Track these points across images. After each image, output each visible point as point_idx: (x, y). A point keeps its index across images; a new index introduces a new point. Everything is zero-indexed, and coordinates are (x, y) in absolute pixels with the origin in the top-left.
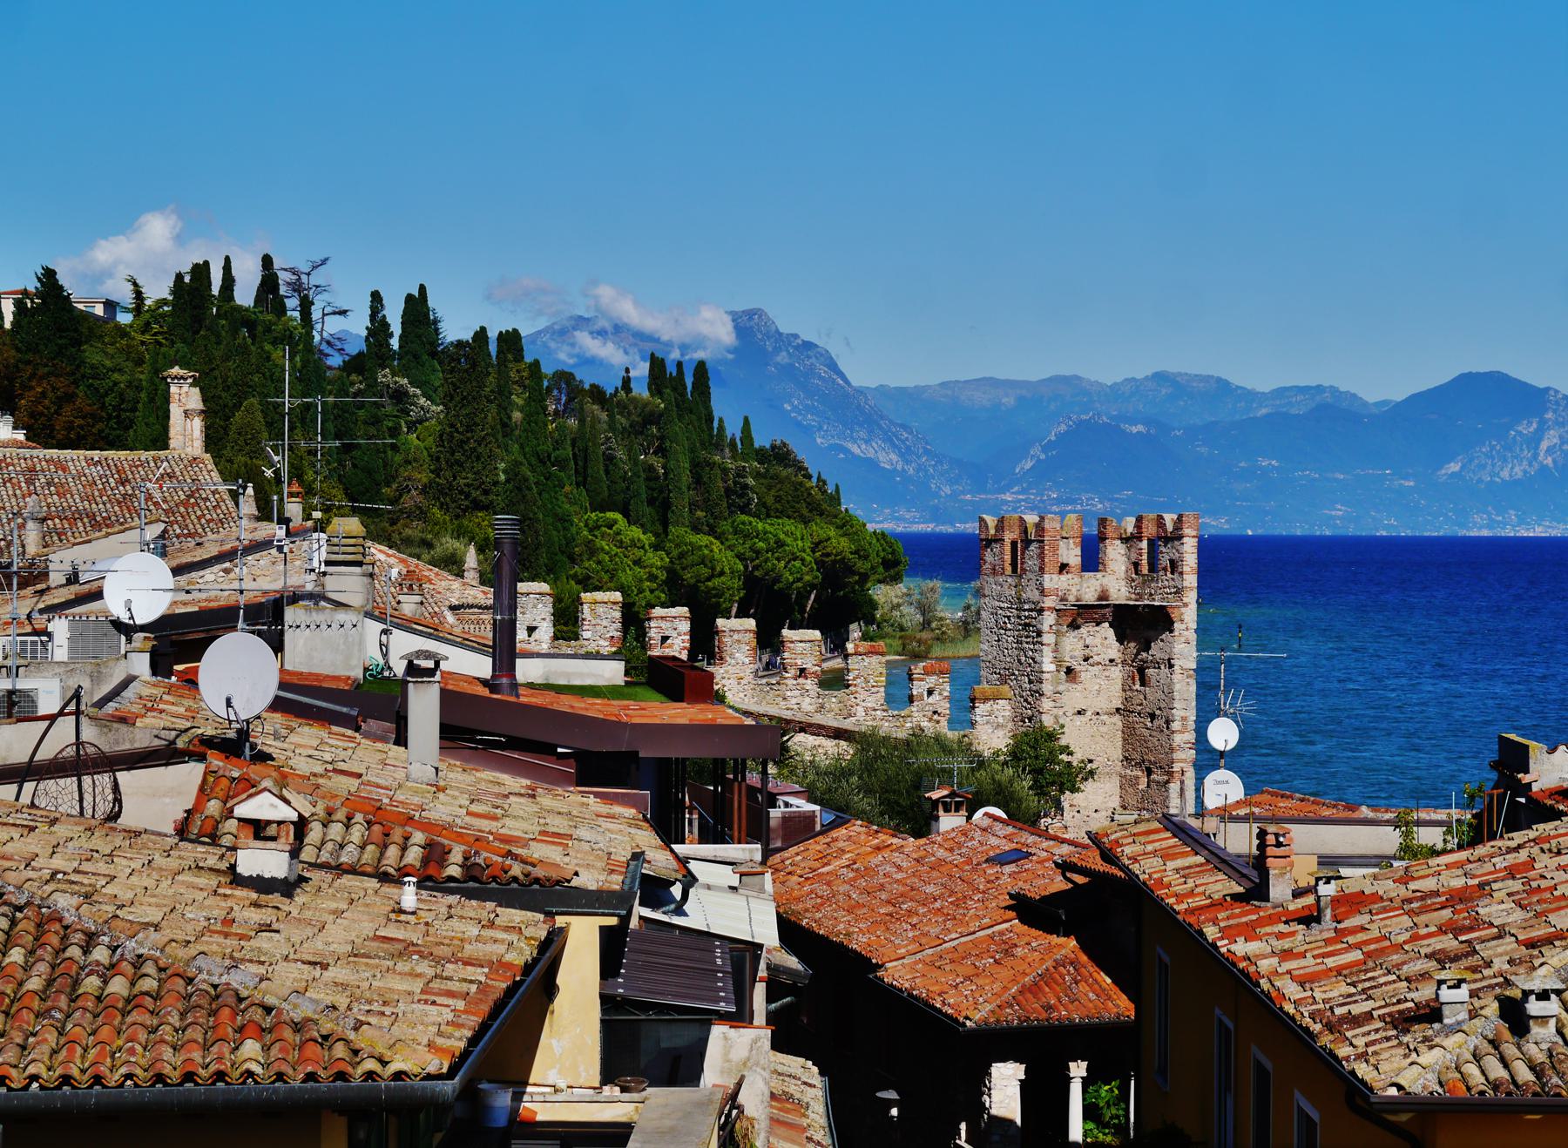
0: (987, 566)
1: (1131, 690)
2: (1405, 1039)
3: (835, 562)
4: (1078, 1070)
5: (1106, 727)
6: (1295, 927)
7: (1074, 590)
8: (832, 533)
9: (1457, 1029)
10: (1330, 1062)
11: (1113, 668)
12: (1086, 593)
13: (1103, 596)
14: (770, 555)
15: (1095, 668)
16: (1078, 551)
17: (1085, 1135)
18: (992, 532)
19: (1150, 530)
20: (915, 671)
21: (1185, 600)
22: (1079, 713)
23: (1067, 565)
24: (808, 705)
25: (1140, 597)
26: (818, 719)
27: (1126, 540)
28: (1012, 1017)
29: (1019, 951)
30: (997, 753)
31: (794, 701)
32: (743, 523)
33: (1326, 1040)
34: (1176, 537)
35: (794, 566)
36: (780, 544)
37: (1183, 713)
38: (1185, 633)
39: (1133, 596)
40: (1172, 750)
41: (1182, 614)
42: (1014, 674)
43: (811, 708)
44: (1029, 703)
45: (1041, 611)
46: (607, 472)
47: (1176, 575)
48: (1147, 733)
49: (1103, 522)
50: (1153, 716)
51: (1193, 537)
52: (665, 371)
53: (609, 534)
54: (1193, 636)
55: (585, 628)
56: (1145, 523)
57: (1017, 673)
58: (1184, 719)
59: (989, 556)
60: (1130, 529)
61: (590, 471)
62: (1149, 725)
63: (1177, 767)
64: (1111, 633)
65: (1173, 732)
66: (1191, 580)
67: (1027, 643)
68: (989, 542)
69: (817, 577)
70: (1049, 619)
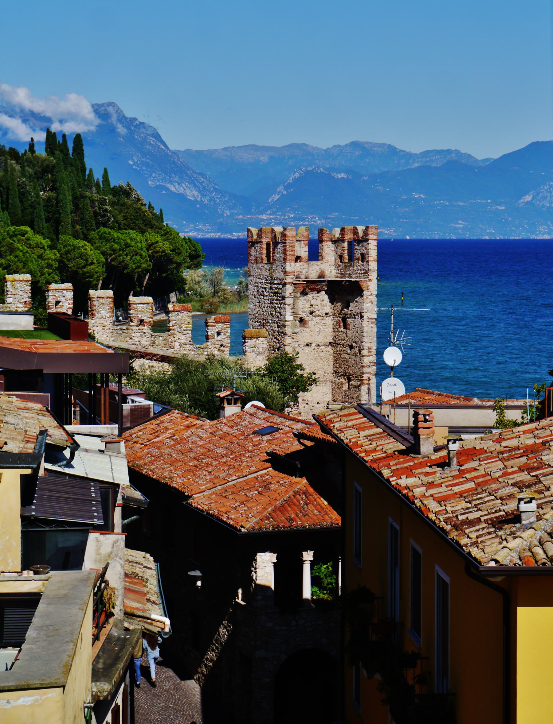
0: (252, 258)
1: (338, 331)
2: (500, 533)
3: (161, 256)
4: (308, 556)
5: (324, 353)
6: (435, 469)
7: (304, 271)
8: (159, 239)
9: (530, 527)
10: (456, 547)
11: (327, 318)
12: (311, 274)
13: (322, 275)
14: (121, 252)
15: (317, 318)
16: (306, 249)
17: (312, 594)
18: (255, 237)
19: (349, 236)
20: (209, 321)
21: (370, 277)
22: (307, 345)
23: (300, 257)
24: (145, 341)
25: (343, 276)
26: (152, 350)
27: (335, 242)
28: (268, 524)
29: (273, 487)
30: (259, 369)
31: (137, 339)
32: (105, 233)
33: (454, 535)
34: (365, 240)
35: (136, 259)
36: (127, 245)
37: (369, 345)
38: (370, 297)
39: (339, 275)
40: (363, 366)
41: (368, 286)
42: (268, 322)
43: (147, 344)
44: (278, 340)
45: (284, 285)
46: (22, 202)
47: (365, 263)
48: (347, 357)
49: (321, 231)
50: (351, 347)
51: (375, 240)
52: (56, 140)
53: (23, 240)
54: (374, 299)
55: (8, 296)
56: (346, 232)
57: (270, 321)
58: (370, 348)
59: (253, 252)
60: (337, 235)
61: (10, 201)
62: (349, 352)
63: (365, 377)
64: (326, 297)
65: (363, 356)
66: (373, 265)
67: (276, 303)
68: (253, 244)
69: (150, 265)
70: (289, 289)
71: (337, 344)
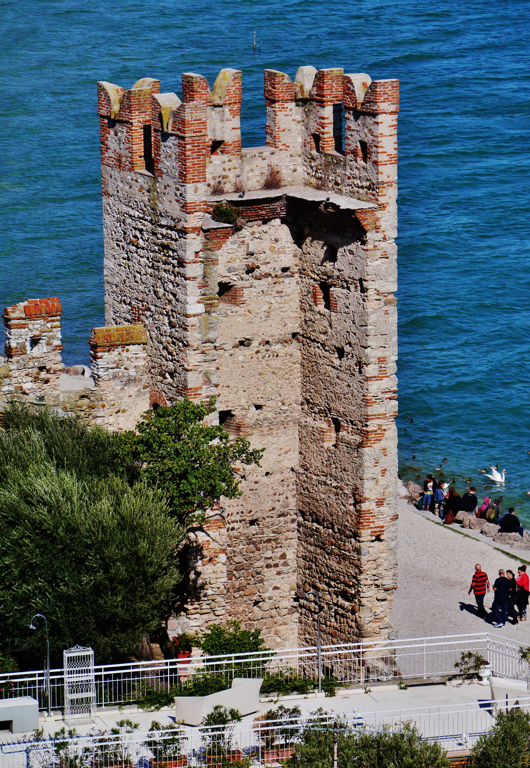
0: (110, 153)
1: (312, 310)
5: (279, 360)
7: (231, 175)
11: (287, 280)
12: (248, 179)
15: (263, 281)
16: (236, 122)
18: (116, 108)
20: (12, 315)
21: (382, 200)
22: (242, 343)
23: (222, 142)
37: (380, 353)
38: (383, 244)
39: (313, 181)
40: (367, 402)
41: (378, 219)
42: (149, 309)
44: (170, 353)
45: (183, 232)
47: (369, 165)
48: (333, 373)
50: (341, 353)
51: (392, 113)
54: (392, 248)
56: (328, 82)
57: (153, 308)
58: (382, 360)
62: (337, 362)
63: (372, 425)
65: (367, 379)
67: (165, 271)
71: (309, 338)
